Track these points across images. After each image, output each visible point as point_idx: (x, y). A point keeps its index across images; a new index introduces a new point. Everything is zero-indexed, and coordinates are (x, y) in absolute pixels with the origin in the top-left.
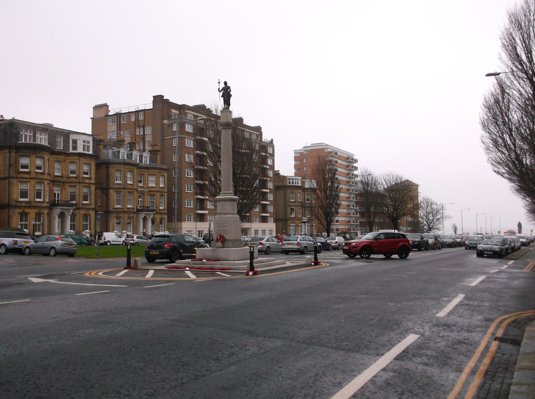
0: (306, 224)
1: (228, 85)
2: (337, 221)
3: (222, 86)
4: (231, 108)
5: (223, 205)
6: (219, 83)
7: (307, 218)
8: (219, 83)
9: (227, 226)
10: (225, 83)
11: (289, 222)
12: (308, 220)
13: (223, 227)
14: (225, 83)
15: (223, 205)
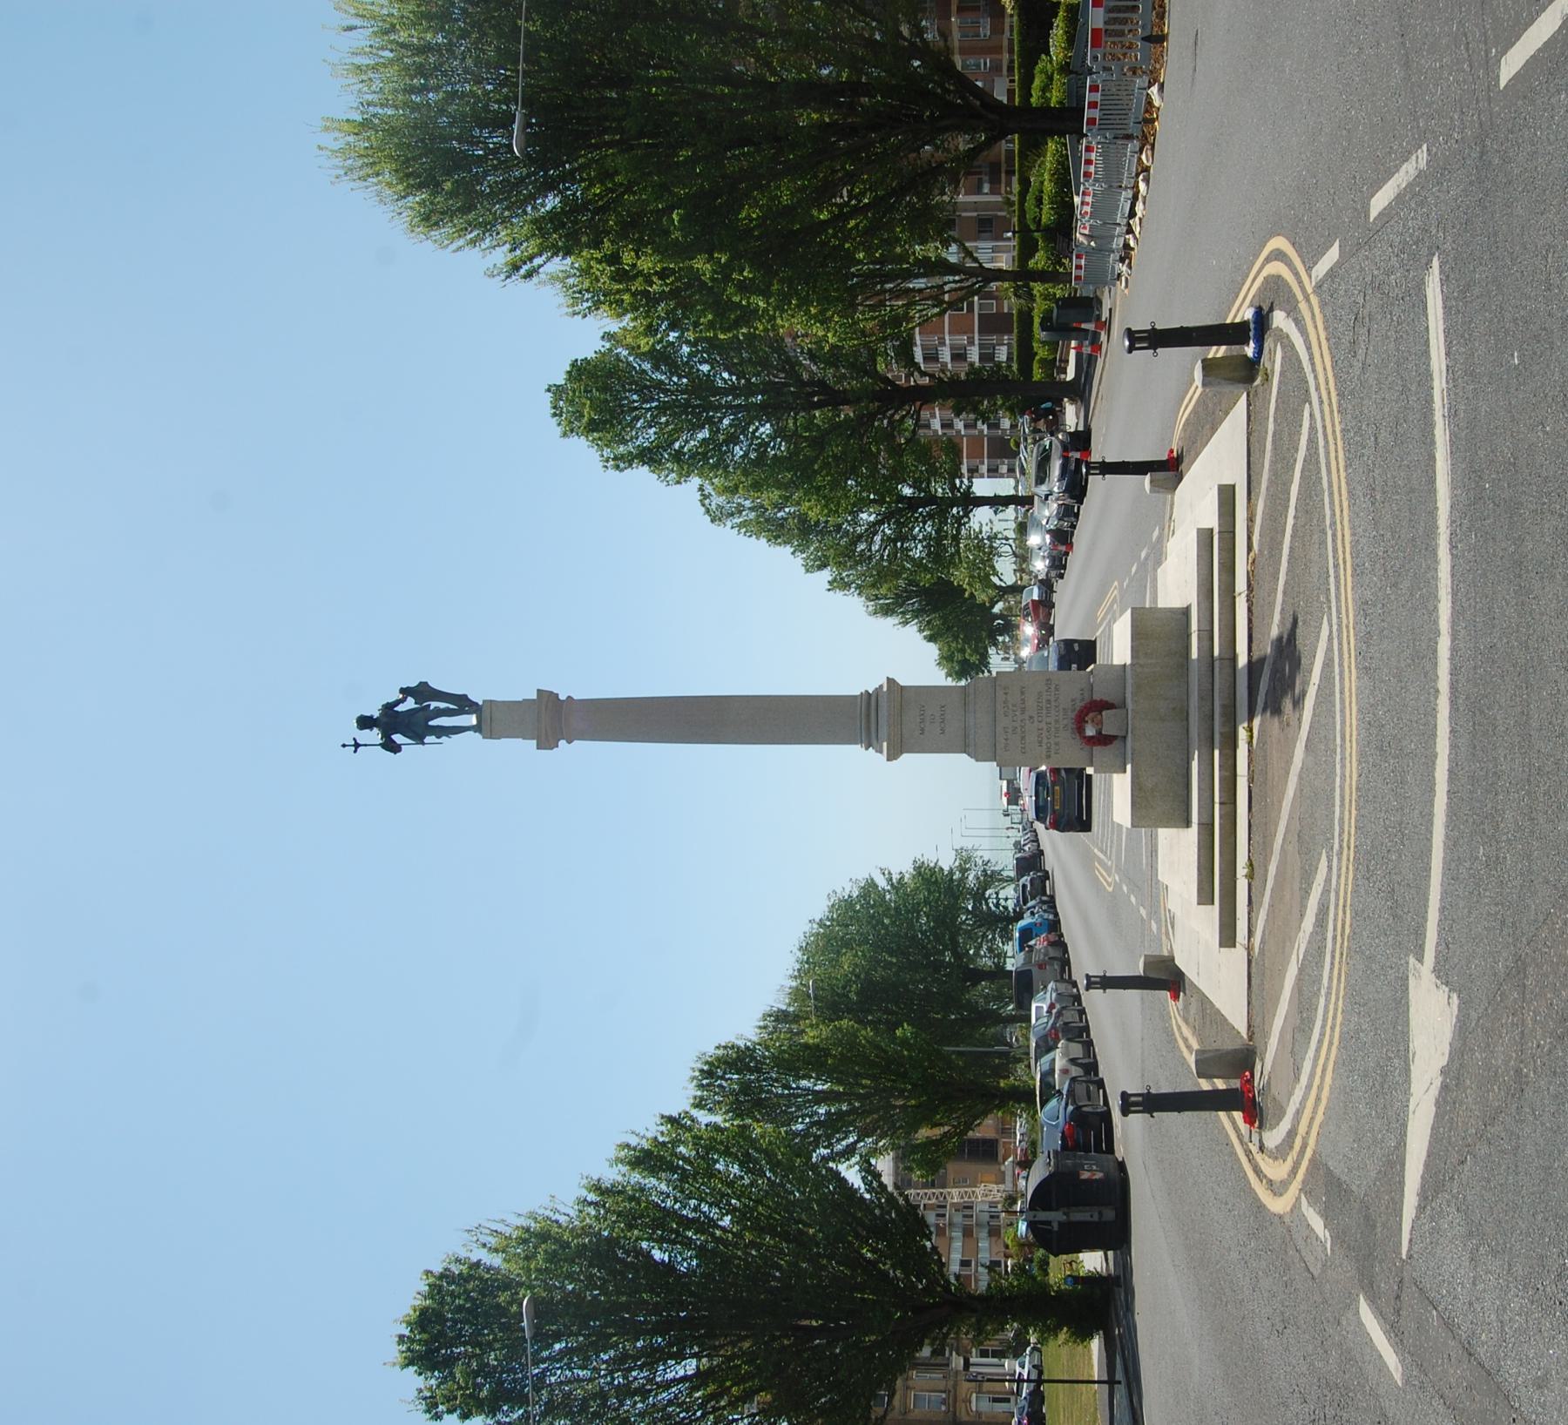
0: (972, 1360)
1: (376, 714)
2: (965, 1264)
3: (374, 735)
4: (477, 697)
5: (923, 721)
6: (357, 745)
7: (951, 1354)
8: (357, 745)
9: (1022, 693)
10: (365, 722)
11: (964, 1418)
12: (958, 1354)
13: (1023, 711)
14: (365, 722)
15: (923, 721)
